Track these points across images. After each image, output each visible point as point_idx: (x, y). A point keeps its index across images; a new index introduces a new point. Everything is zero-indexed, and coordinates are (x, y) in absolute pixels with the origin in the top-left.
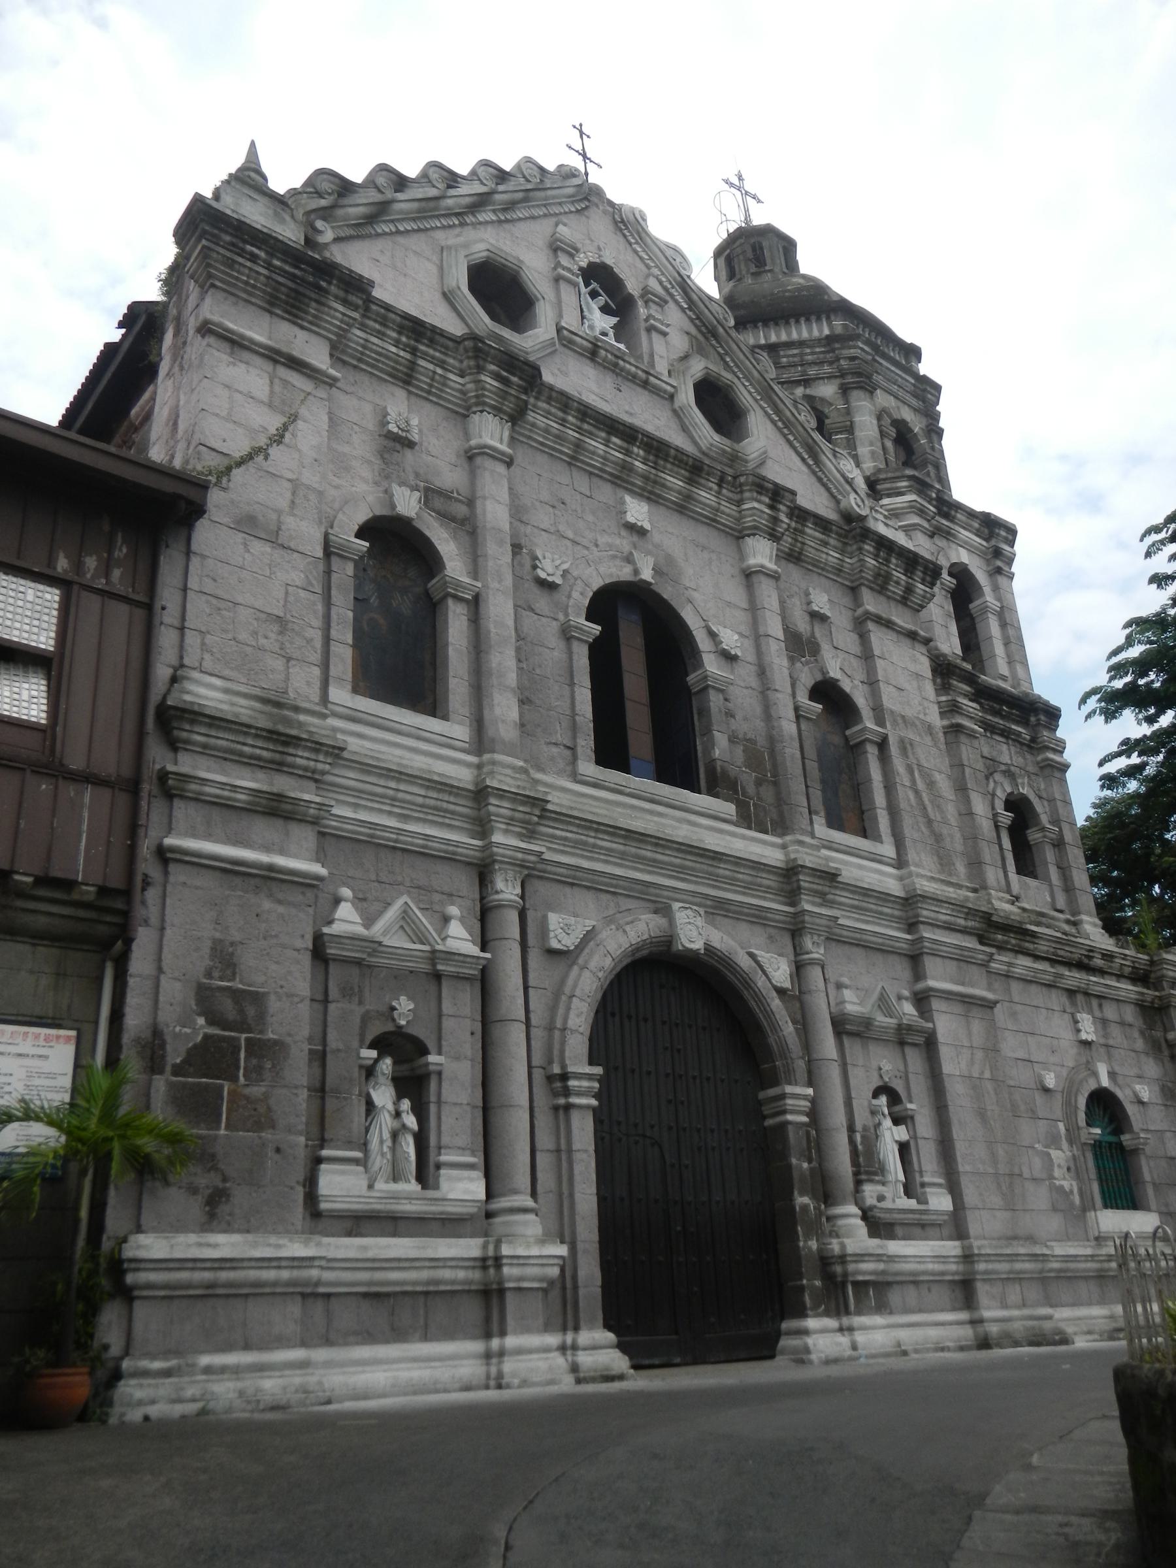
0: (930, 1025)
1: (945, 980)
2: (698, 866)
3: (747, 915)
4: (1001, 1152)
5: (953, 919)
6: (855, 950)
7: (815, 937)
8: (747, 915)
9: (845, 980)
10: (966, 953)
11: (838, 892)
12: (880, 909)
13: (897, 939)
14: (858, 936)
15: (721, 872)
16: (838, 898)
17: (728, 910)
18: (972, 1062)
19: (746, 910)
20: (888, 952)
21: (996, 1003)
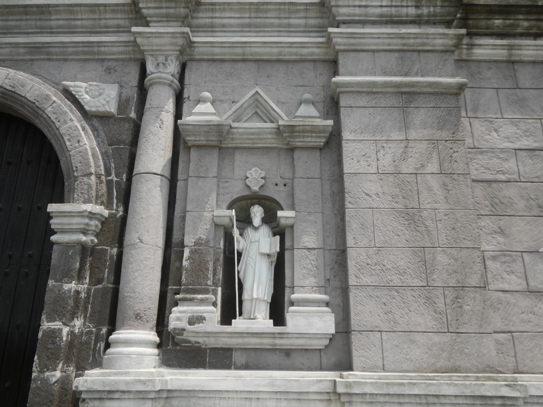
0: (330, 122)
1: (366, 74)
2: (23, 23)
3: (77, 53)
4: (442, 259)
5: (393, 9)
6: (240, 65)
7: (161, 59)
8: (77, 53)
9: (207, 94)
10: (412, 41)
11: (218, 15)
12: (286, 21)
13: (302, 45)
14: (239, 50)
15: (53, 23)
16: (217, 21)
17: (48, 54)
18: (404, 156)
19: (71, 49)
20: (295, 61)
21: (462, 87)
